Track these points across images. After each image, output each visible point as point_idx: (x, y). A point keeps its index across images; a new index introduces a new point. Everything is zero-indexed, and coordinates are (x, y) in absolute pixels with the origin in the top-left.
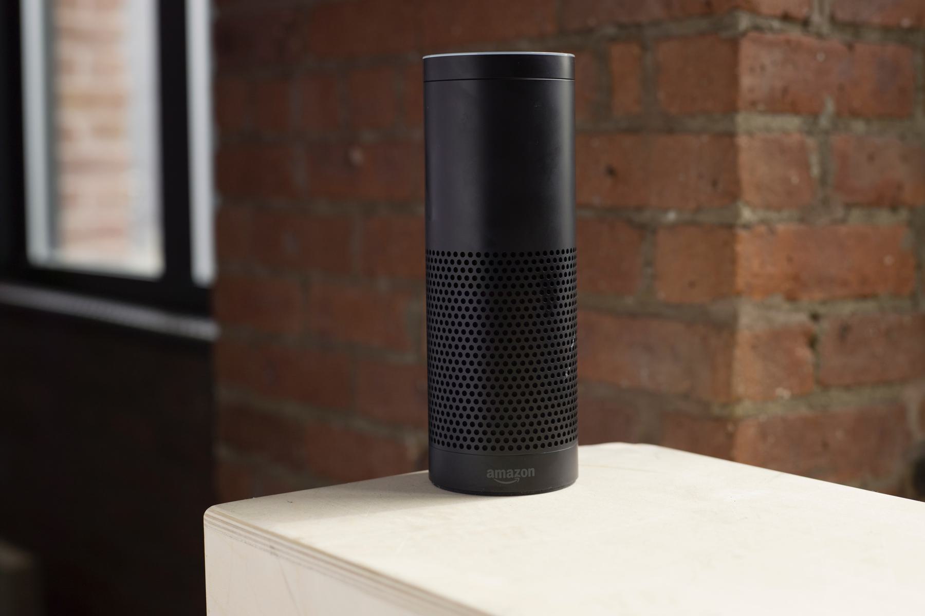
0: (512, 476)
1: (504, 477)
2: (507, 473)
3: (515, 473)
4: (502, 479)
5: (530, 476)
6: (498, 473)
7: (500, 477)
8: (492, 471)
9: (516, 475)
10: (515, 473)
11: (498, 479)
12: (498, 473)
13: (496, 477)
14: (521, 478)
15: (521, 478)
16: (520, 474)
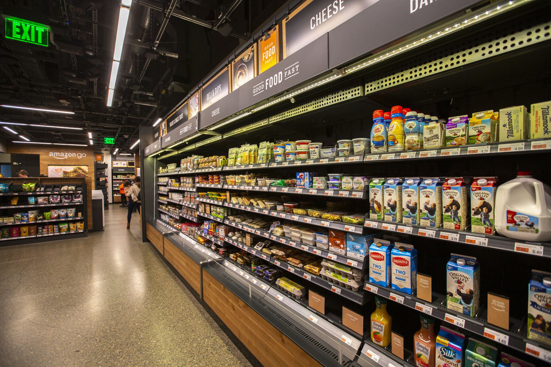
0: (63, 156)
1: (59, 156)
2: (60, 154)
3: (65, 154)
4: (58, 157)
5: (73, 156)
6: (56, 154)
7: (57, 156)
8: (52, 153)
9: (66, 155)
10: (65, 154)
11: (56, 156)
12: (56, 154)
13: (55, 156)
14: (68, 157)
15: (68, 157)
16: (68, 155)
